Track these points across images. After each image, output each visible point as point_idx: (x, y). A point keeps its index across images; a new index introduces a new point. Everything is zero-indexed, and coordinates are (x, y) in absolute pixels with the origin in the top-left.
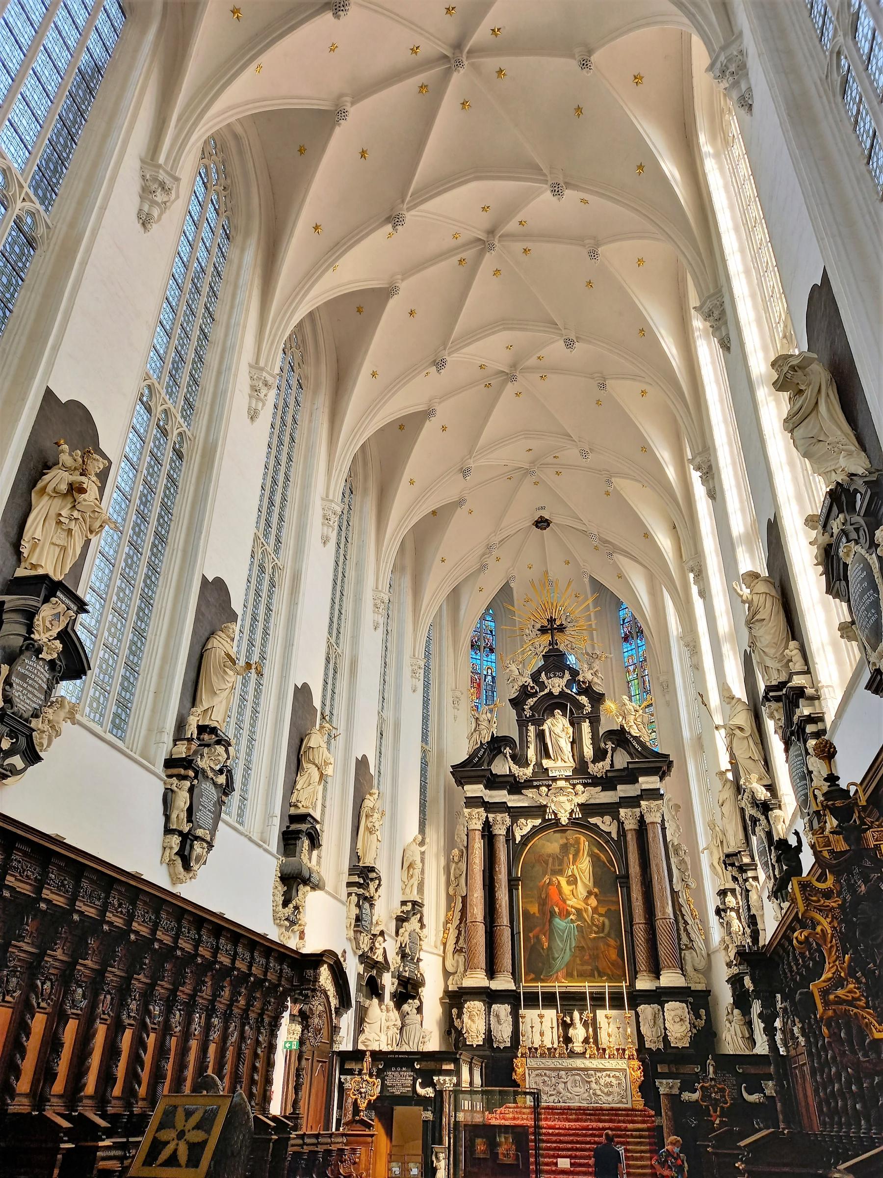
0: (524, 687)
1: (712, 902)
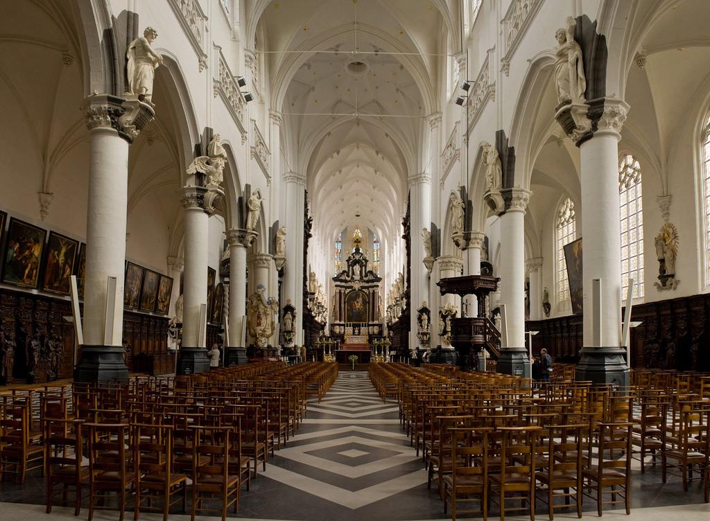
0: (350, 258)
1: (386, 309)
